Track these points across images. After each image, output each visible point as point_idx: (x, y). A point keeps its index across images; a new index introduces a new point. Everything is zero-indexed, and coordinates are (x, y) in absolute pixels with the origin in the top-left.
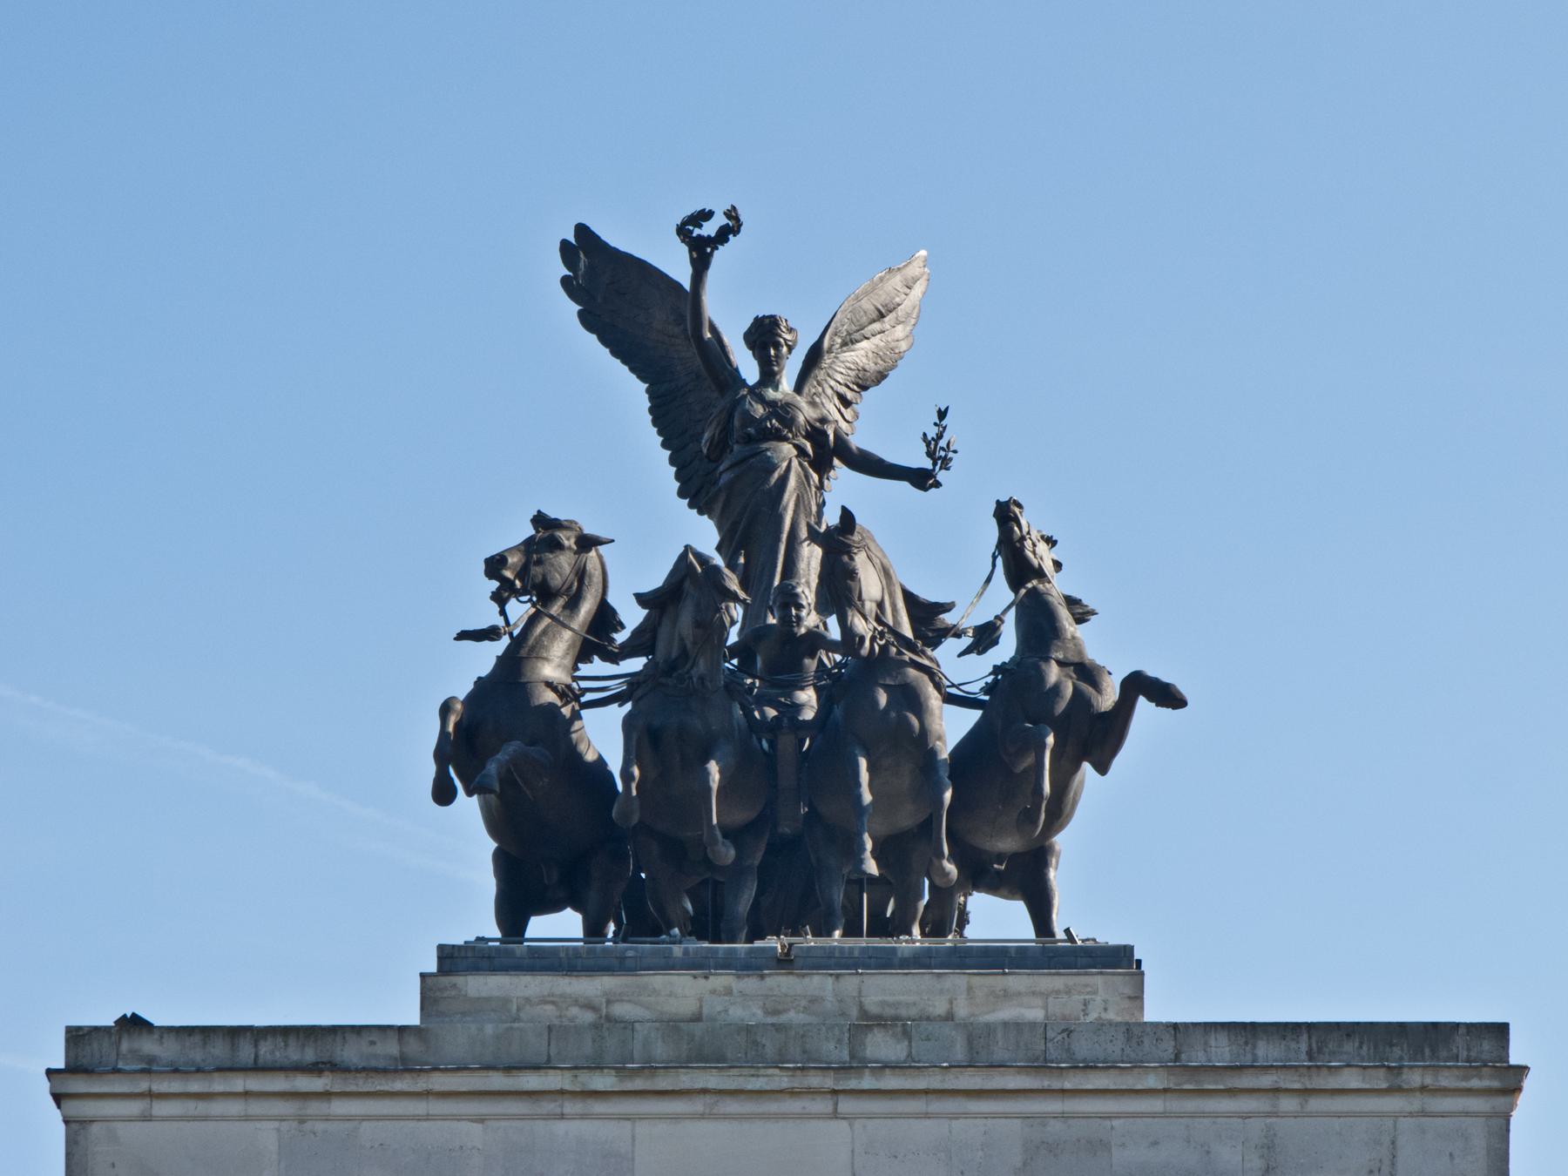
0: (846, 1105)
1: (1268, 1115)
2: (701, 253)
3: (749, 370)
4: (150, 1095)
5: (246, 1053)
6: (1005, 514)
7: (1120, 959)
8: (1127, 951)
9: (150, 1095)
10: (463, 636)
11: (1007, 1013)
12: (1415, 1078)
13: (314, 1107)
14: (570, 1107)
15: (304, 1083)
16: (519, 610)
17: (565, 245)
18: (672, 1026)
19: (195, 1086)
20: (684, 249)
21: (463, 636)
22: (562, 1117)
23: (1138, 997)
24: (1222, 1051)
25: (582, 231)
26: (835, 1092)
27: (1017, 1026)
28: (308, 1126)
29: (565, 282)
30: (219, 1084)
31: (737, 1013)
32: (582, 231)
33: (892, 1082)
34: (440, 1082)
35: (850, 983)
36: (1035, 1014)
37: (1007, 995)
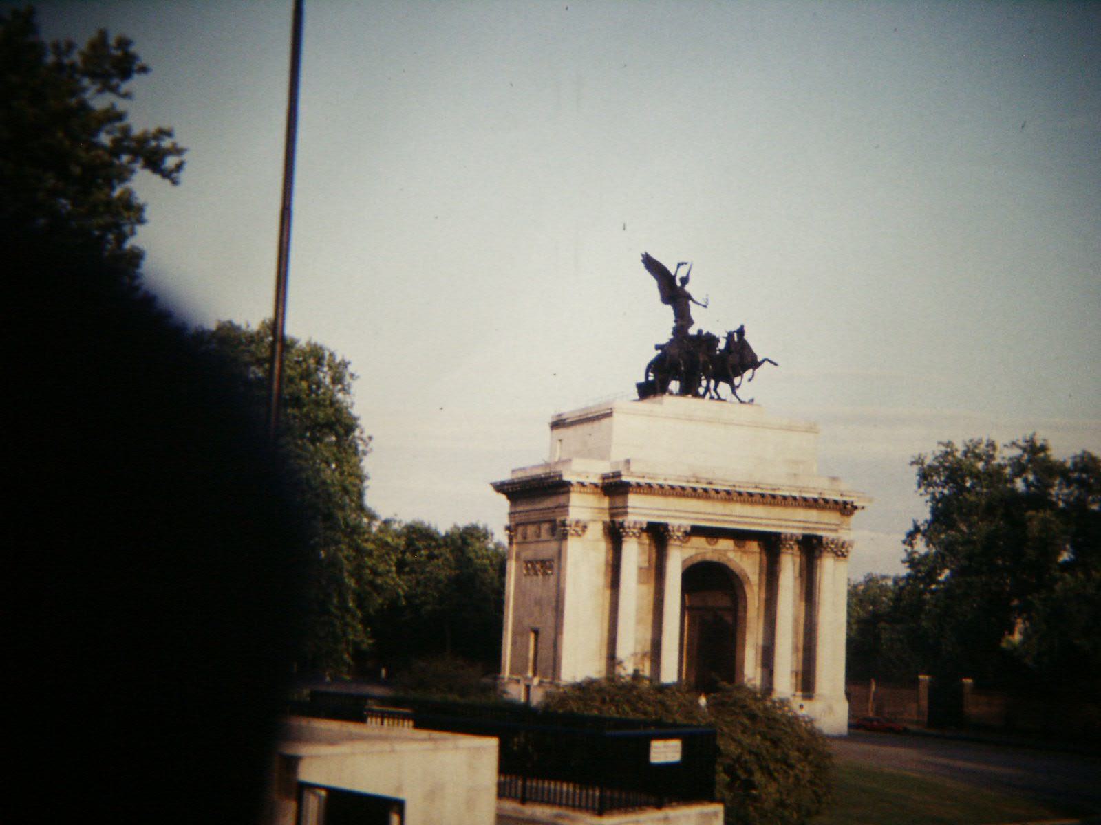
6: (742, 327)
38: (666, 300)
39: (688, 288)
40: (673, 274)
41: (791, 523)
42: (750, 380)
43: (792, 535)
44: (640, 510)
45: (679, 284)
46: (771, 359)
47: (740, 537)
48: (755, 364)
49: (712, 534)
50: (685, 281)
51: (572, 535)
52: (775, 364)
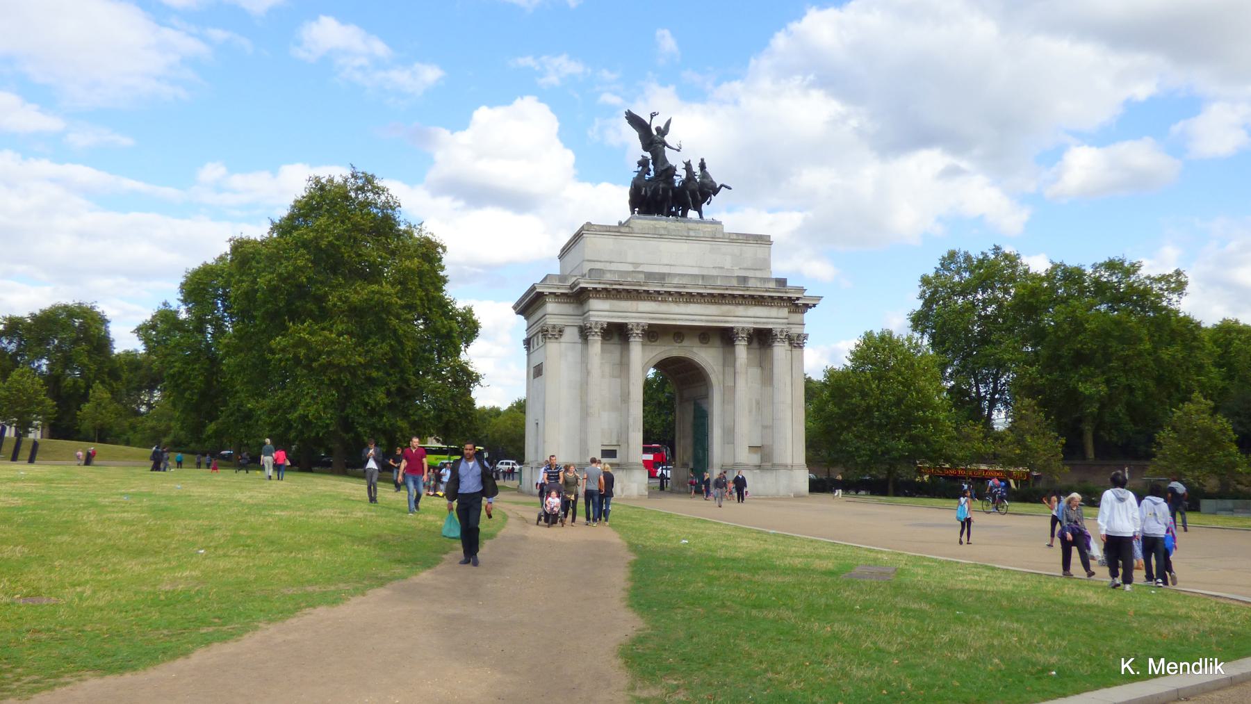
0: (687, 241)
2: (652, 118)
3: (655, 133)
5: (608, 229)
6: (702, 160)
7: (720, 223)
8: (721, 222)
11: (706, 229)
12: (759, 242)
14: (651, 239)
16: (641, 168)
18: (665, 228)
23: (723, 228)
24: (735, 237)
27: (708, 231)
31: (672, 227)
32: (629, 110)
33: (694, 238)
35: (686, 224)
36: (709, 230)
37: (707, 227)
38: (645, 149)
39: (667, 139)
40: (649, 123)
41: (744, 318)
42: (708, 204)
43: (743, 329)
44: (602, 311)
45: (655, 133)
46: (725, 184)
47: (705, 334)
48: (716, 191)
49: (678, 333)
50: (663, 132)
51: (549, 338)
52: (730, 189)
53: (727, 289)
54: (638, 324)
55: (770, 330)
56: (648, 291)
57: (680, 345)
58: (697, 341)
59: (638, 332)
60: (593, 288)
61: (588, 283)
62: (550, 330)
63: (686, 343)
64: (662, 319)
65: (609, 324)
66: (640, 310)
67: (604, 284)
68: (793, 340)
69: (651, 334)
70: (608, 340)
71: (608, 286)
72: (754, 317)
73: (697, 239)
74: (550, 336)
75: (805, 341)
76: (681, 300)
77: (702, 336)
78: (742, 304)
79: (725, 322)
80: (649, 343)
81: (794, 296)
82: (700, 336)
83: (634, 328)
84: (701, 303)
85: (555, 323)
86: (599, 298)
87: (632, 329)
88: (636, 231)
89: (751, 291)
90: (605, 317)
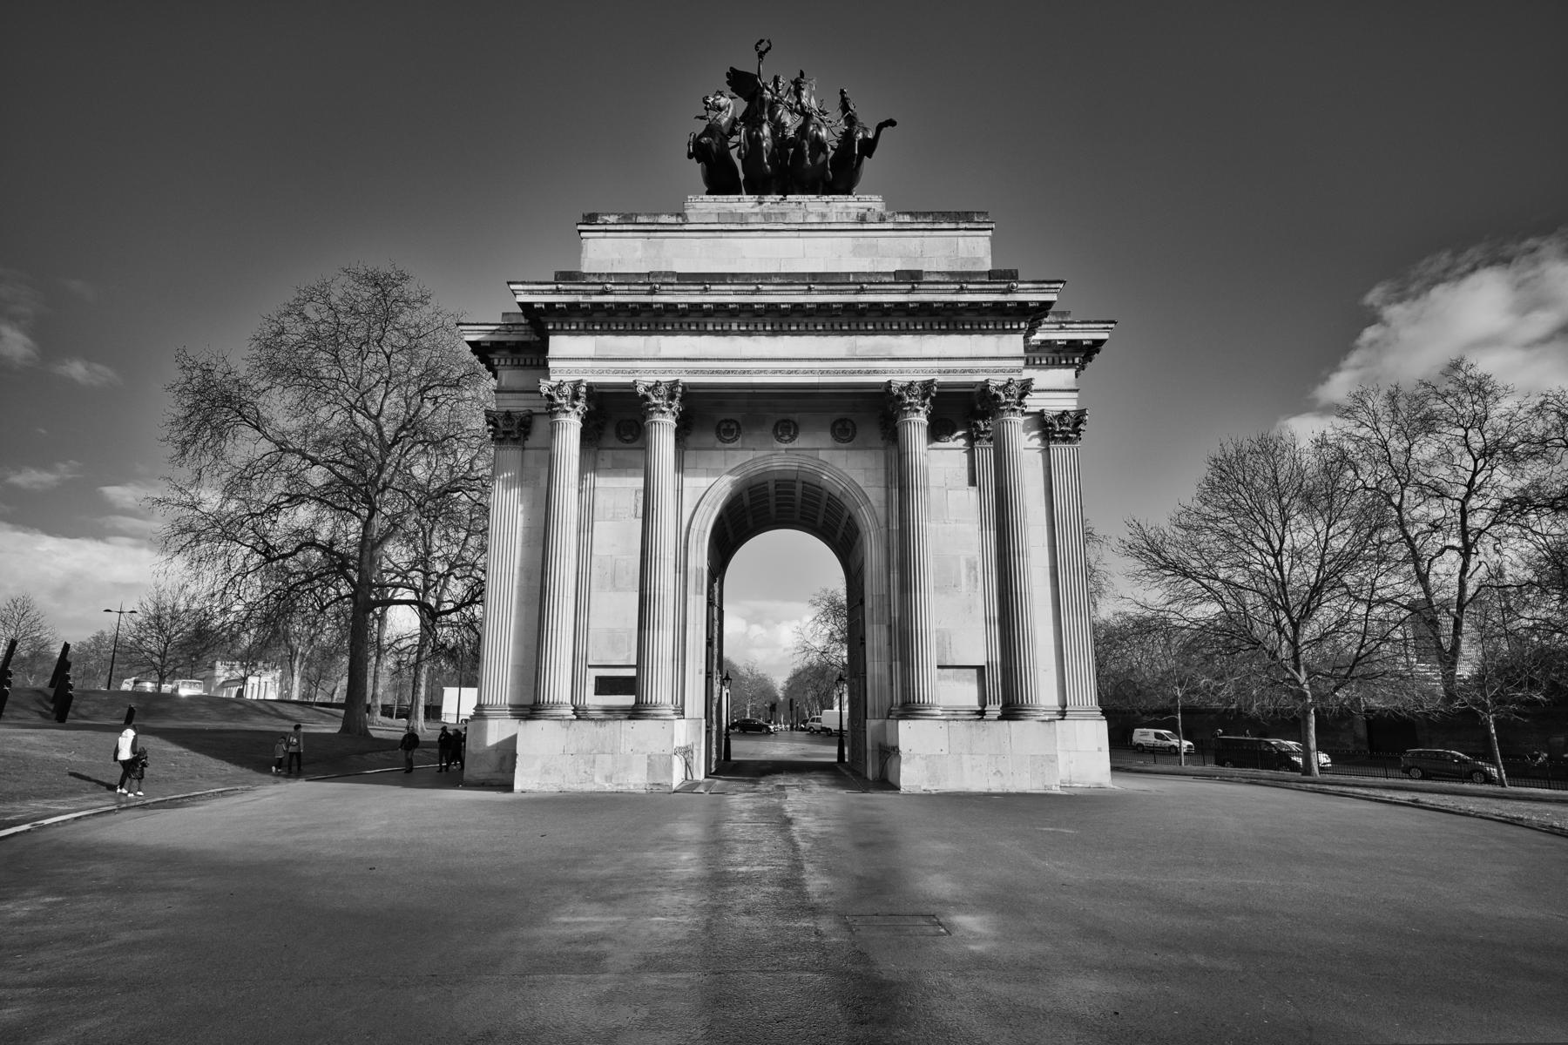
0: (802, 234)
1: (922, 237)
2: (761, 55)
4: (606, 231)
6: (842, 92)
9: (606, 231)
10: (697, 117)
13: (652, 234)
14: (724, 234)
15: (649, 227)
17: (728, 74)
19: (618, 228)
20: (757, 53)
21: (697, 117)
22: (721, 237)
25: (731, 68)
26: (799, 230)
28: (651, 240)
29: (728, 82)
30: (625, 227)
32: (731, 68)
33: (815, 227)
34: (687, 227)
48: (869, 147)
52: (891, 123)
53: (862, 291)
54: (657, 384)
55: (985, 385)
56: (675, 305)
57: (790, 445)
58: (826, 438)
59: (660, 401)
60: (546, 304)
61: (531, 292)
62: (500, 423)
63: (800, 442)
64: (718, 372)
65: (590, 387)
66: (664, 354)
67: (568, 292)
68: (1051, 425)
69: (724, 426)
70: (628, 441)
71: (581, 298)
72: (939, 359)
73: (824, 228)
74: (502, 436)
75: (1081, 427)
76: (760, 327)
77: (839, 426)
78: (907, 331)
79: (868, 373)
80: (719, 444)
81: (1034, 298)
82: (834, 425)
83: (650, 394)
84: (807, 332)
85: (511, 409)
86: (570, 333)
87: (646, 398)
88: (691, 220)
89: (927, 291)
90: (585, 371)
